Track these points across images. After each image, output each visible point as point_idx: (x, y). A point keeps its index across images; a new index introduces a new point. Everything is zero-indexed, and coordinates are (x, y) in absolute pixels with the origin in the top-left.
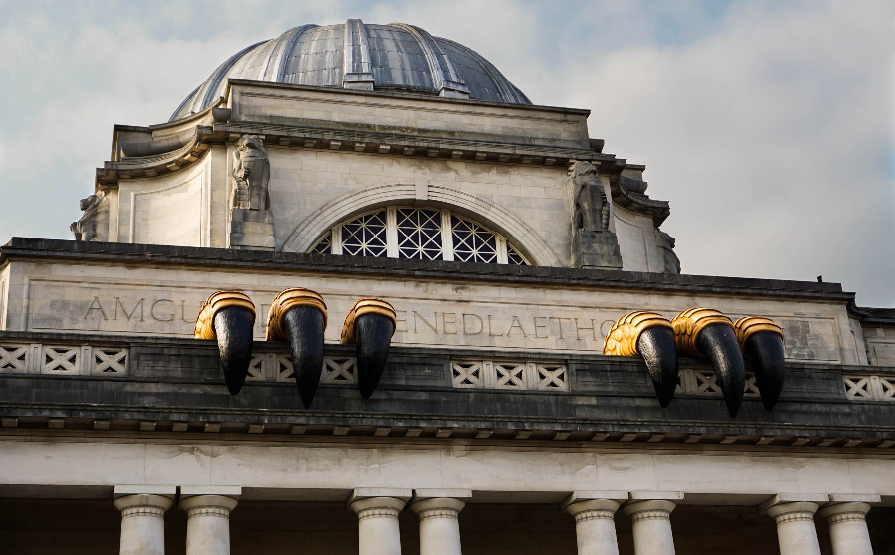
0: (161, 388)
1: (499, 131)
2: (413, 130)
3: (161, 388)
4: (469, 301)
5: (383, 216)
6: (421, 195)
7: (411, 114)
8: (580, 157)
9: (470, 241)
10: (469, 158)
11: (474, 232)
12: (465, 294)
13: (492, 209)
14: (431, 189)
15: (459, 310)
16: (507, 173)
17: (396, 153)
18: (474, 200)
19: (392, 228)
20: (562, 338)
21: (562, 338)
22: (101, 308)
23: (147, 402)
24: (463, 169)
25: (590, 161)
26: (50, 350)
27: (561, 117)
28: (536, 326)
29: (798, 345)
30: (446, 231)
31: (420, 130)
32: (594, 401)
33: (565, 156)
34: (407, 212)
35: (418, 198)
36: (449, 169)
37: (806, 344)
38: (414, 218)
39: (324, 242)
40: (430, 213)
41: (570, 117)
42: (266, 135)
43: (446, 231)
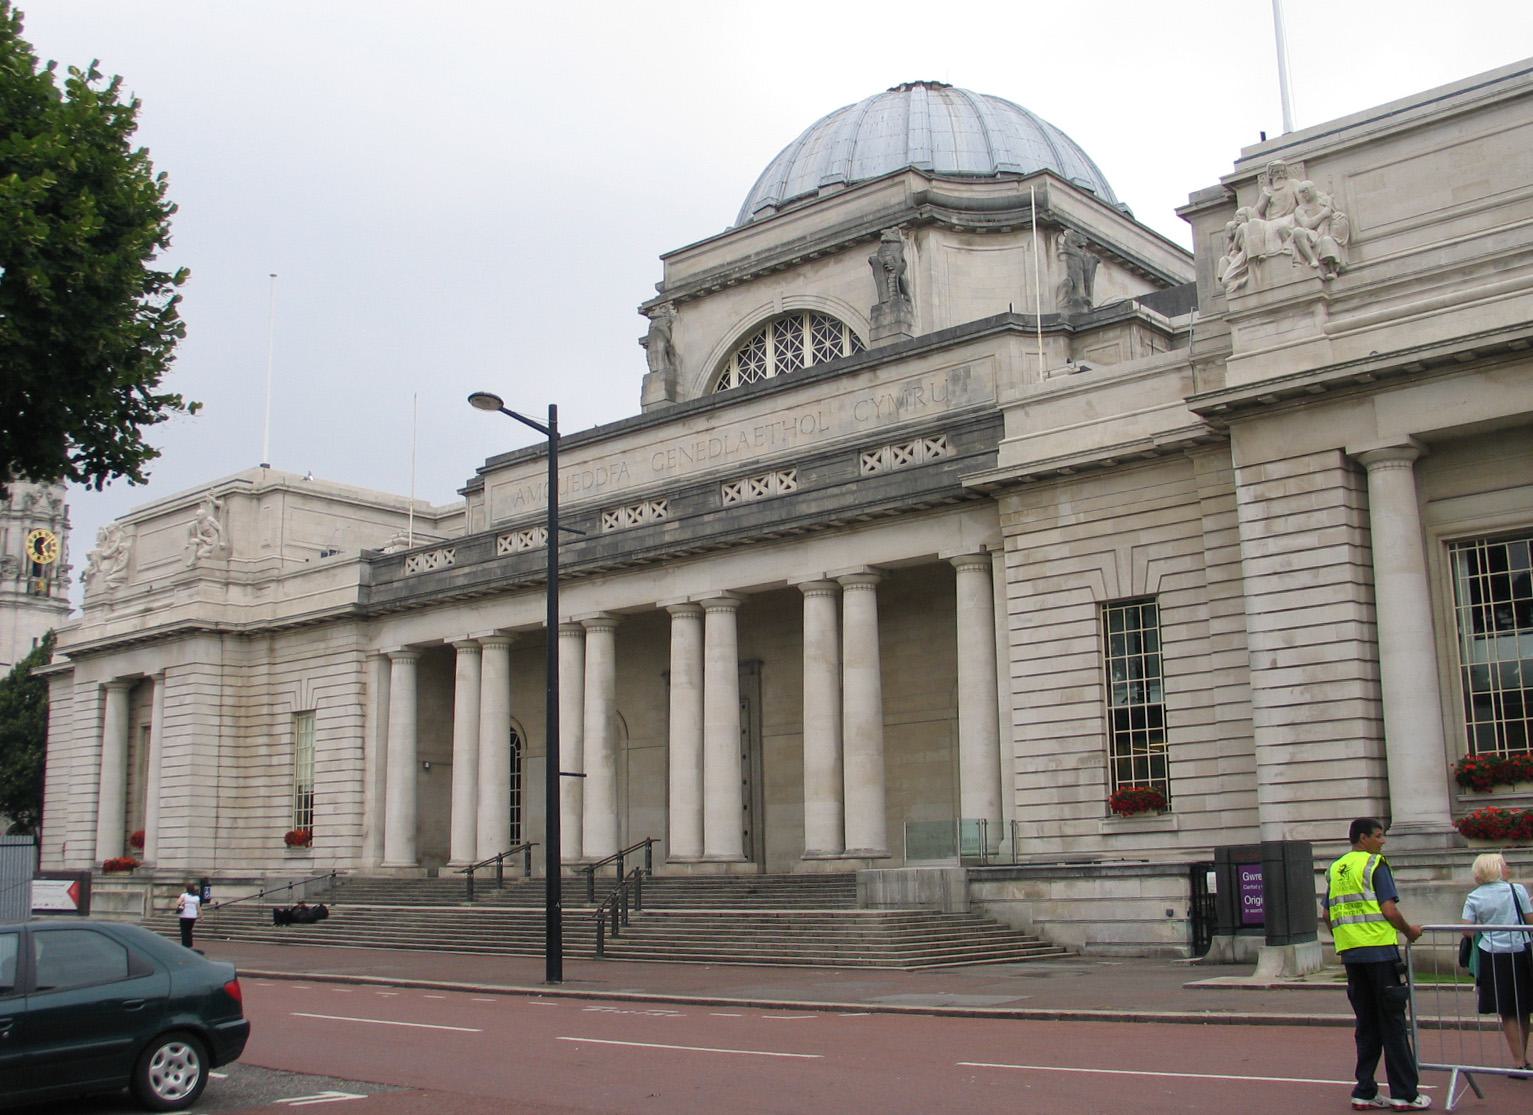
0: (467, 570)
1: (841, 219)
2: (777, 247)
3: (467, 570)
4: (714, 428)
5: (764, 334)
6: (778, 310)
7: (778, 231)
8: (887, 225)
9: (824, 336)
10: (807, 260)
11: (827, 325)
12: (714, 423)
13: (828, 302)
14: (784, 301)
15: (706, 437)
16: (841, 261)
17: (757, 277)
18: (815, 299)
19: (770, 343)
20: (773, 443)
21: (773, 443)
22: (522, 497)
23: (460, 582)
24: (807, 269)
25: (897, 225)
26: (427, 556)
27: (889, 182)
28: (756, 436)
29: (957, 393)
30: (807, 333)
31: (784, 245)
32: (676, 525)
33: (875, 229)
34: (780, 324)
35: (776, 312)
36: (799, 275)
37: (966, 390)
38: (786, 329)
39: (721, 375)
40: (796, 319)
41: (897, 179)
42: (674, 300)
43: (807, 333)
